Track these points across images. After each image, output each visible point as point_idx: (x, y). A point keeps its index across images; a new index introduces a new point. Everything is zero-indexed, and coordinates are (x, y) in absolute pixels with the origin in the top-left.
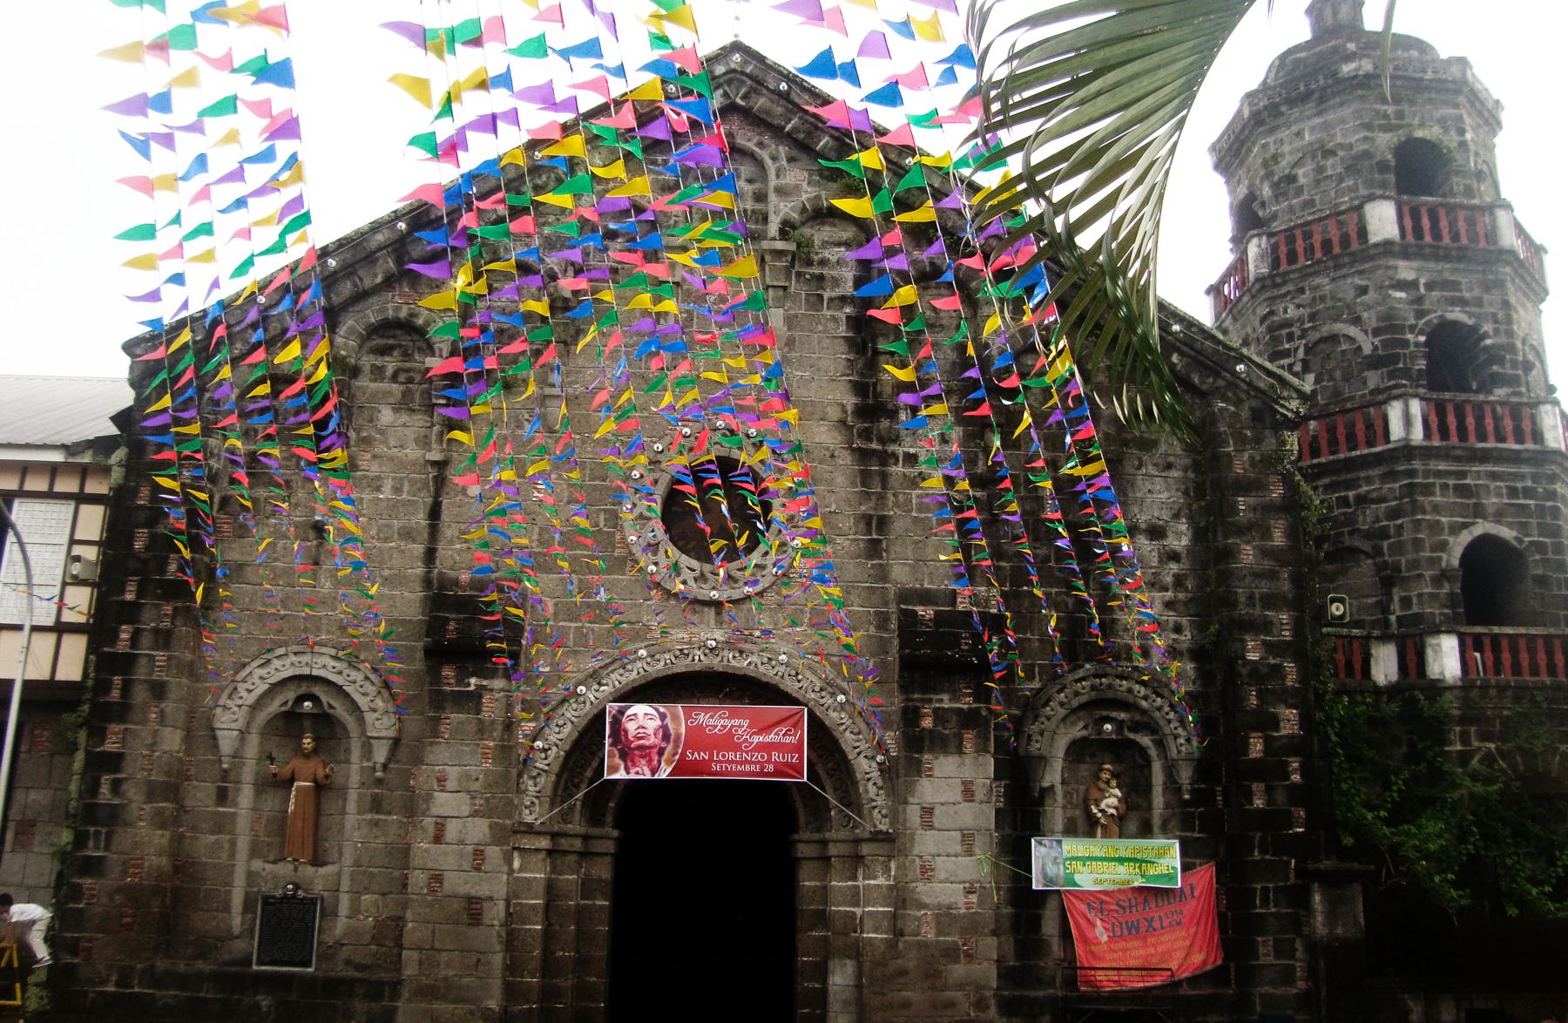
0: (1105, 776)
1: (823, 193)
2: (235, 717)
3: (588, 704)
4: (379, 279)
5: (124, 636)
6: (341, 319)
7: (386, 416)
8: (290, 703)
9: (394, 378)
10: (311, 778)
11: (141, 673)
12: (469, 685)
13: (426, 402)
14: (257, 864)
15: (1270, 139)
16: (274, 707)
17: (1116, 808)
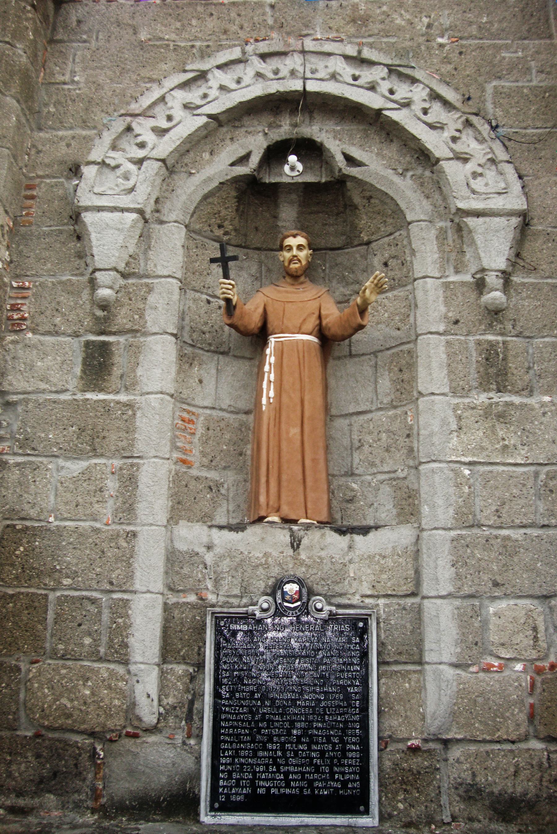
8: (255, 160)
10: (312, 323)
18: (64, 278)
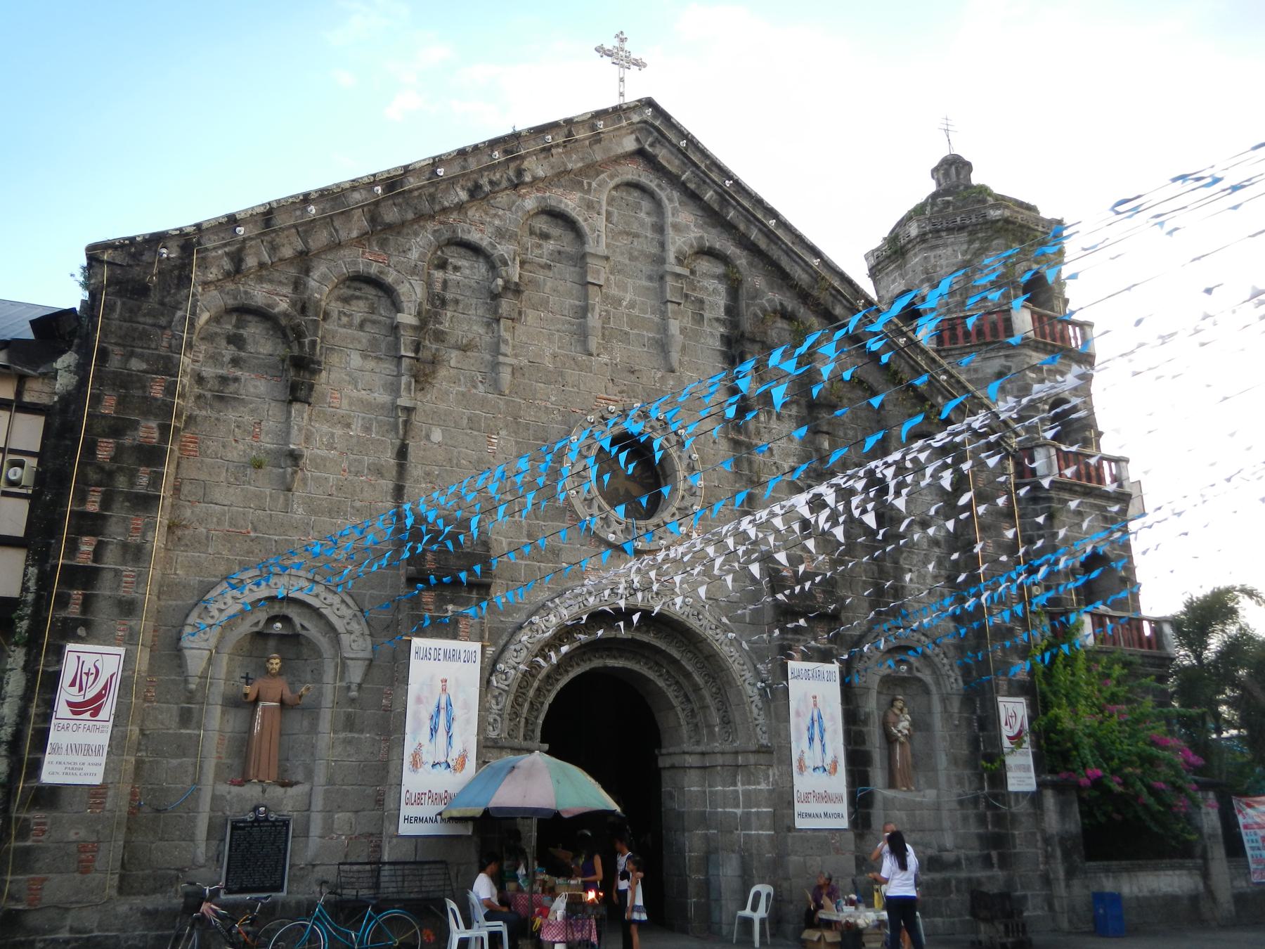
0: (899, 704)
1: (705, 235)
2: (207, 636)
4: (355, 234)
5: (84, 548)
6: (315, 263)
7: (356, 360)
8: (262, 624)
9: (361, 326)
10: (279, 697)
11: (105, 589)
12: (447, 611)
13: (393, 353)
14: (223, 788)
15: (932, 254)
16: (246, 627)
17: (909, 730)
18: (173, 677)
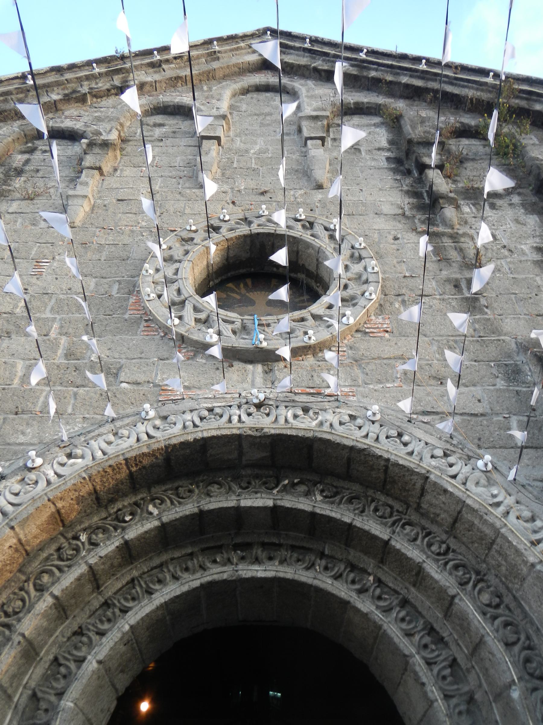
3: (42, 484)
